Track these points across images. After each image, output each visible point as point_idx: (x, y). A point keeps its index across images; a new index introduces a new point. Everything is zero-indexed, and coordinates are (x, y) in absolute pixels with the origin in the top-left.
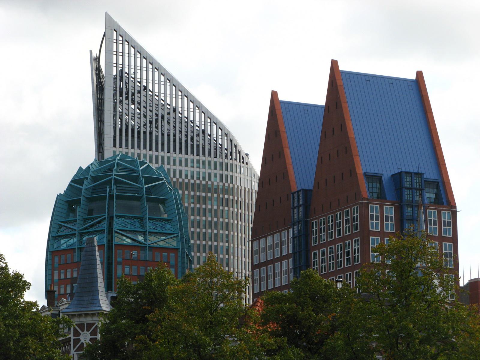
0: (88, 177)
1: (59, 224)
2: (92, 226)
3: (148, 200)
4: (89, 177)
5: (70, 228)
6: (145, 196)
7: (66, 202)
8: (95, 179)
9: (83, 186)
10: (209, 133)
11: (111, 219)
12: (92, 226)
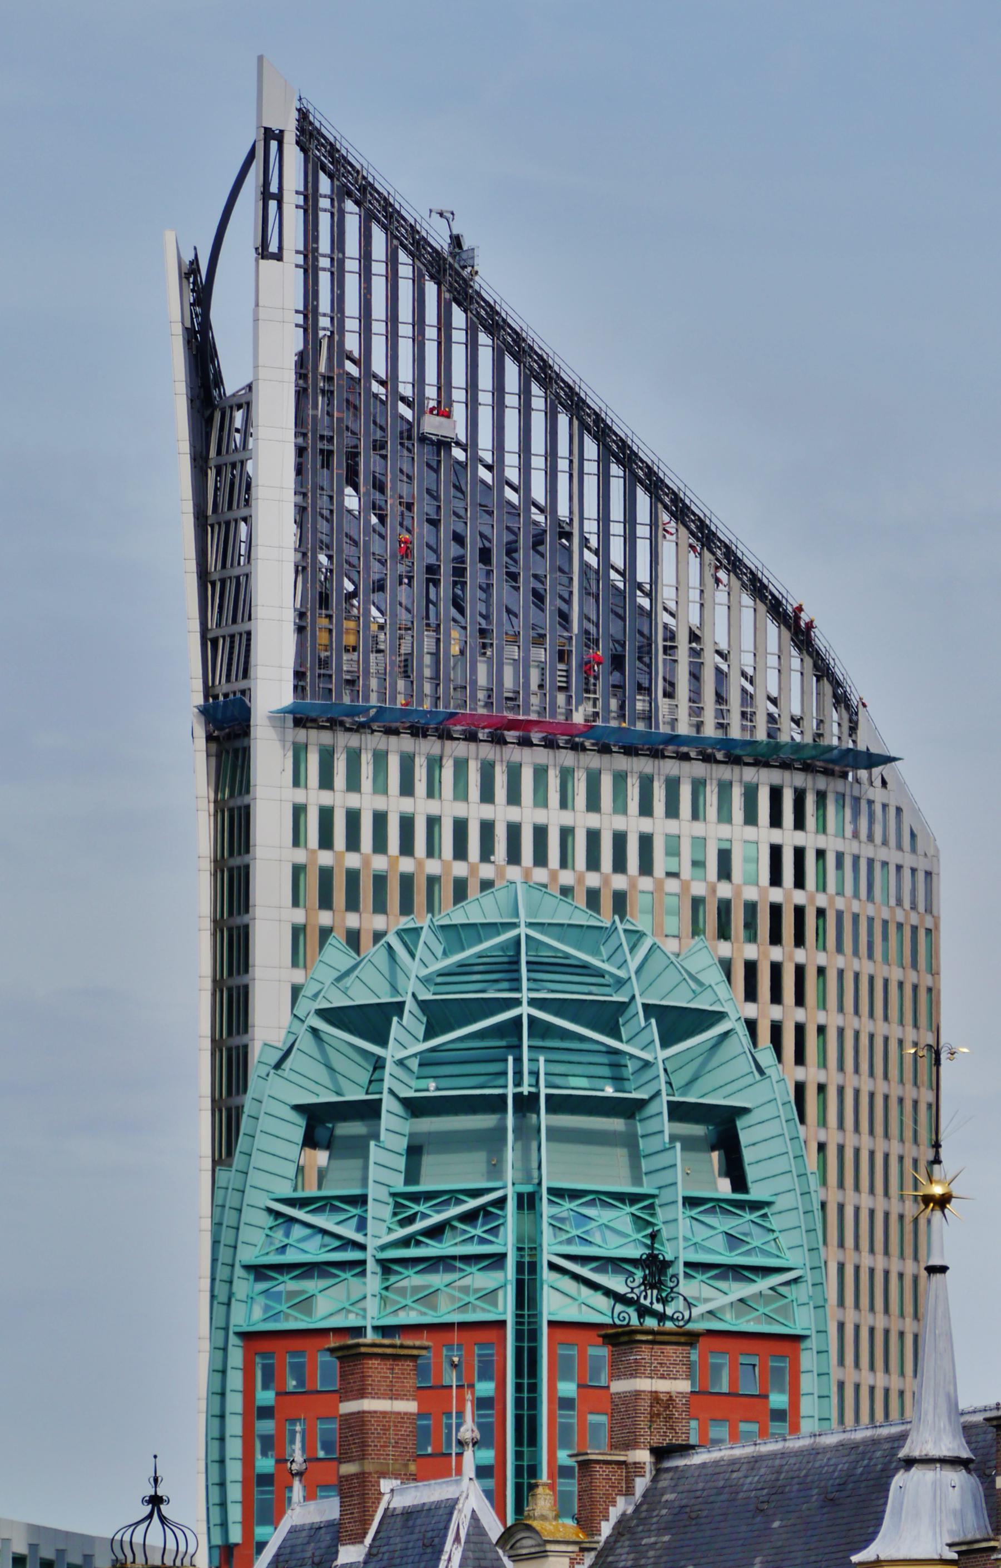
0: (404, 1003)
1: (270, 1211)
2: (436, 1232)
3: (679, 1112)
4: (410, 1005)
5: (324, 1232)
6: (665, 1098)
7: (298, 1108)
8: (438, 1017)
9: (383, 1042)
10: (723, 646)
11: (528, 1202)
12: (436, 1232)
